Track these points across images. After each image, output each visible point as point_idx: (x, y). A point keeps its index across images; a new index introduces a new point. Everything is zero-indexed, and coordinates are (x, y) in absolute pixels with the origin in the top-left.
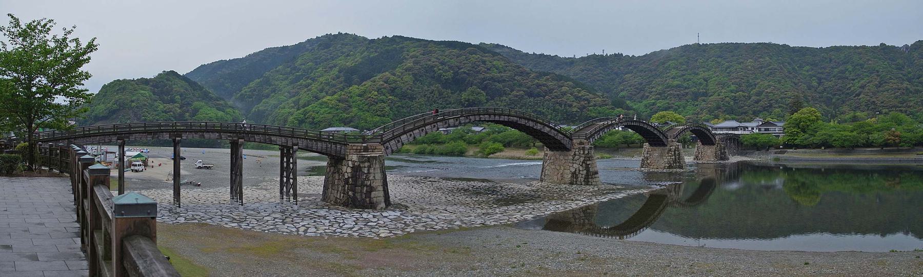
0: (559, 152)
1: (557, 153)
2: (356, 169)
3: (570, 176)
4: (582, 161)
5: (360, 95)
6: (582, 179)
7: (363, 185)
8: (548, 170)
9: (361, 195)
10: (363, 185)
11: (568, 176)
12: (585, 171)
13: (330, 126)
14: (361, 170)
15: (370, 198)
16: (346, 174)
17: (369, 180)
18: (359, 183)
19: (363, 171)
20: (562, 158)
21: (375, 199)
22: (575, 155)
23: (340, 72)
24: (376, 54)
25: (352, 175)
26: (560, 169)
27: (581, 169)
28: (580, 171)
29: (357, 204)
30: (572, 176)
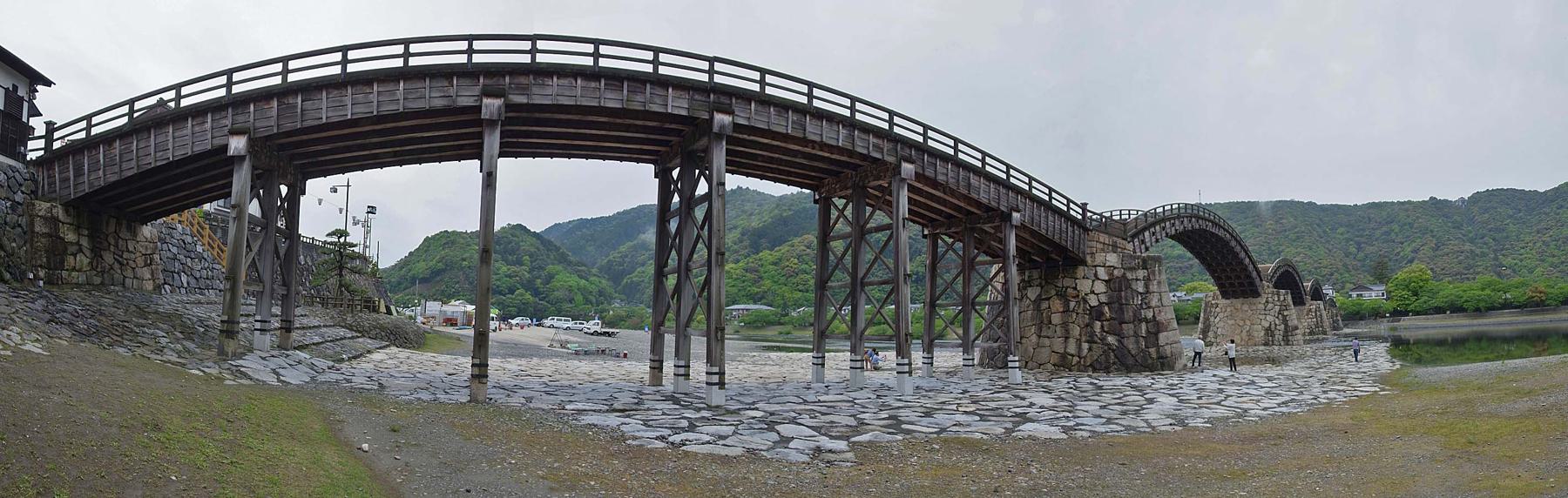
0: (1241, 299)
1: (1237, 302)
2: (1117, 285)
3: (1263, 333)
4: (1277, 310)
5: (775, 264)
6: (1281, 337)
7: (1138, 319)
8: (1223, 328)
9: (1137, 342)
10: (1138, 319)
11: (1260, 334)
12: (1283, 326)
13: (734, 304)
14: (1129, 287)
15: (1157, 346)
16: (1092, 297)
17: (1149, 307)
18: (1129, 315)
19: (1134, 287)
20: (1246, 307)
21: (1168, 348)
22: (1267, 302)
23: (743, 234)
24: (790, 213)
25: (1110, 297)
26: (1245, 324)
27: (1277, 323)
28: (1276, 325)
29: (1130, 361)
30: (1266, 334)
